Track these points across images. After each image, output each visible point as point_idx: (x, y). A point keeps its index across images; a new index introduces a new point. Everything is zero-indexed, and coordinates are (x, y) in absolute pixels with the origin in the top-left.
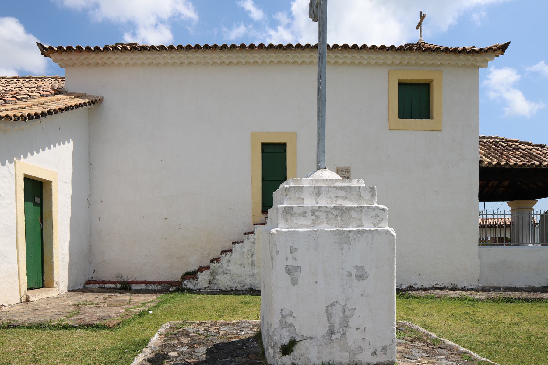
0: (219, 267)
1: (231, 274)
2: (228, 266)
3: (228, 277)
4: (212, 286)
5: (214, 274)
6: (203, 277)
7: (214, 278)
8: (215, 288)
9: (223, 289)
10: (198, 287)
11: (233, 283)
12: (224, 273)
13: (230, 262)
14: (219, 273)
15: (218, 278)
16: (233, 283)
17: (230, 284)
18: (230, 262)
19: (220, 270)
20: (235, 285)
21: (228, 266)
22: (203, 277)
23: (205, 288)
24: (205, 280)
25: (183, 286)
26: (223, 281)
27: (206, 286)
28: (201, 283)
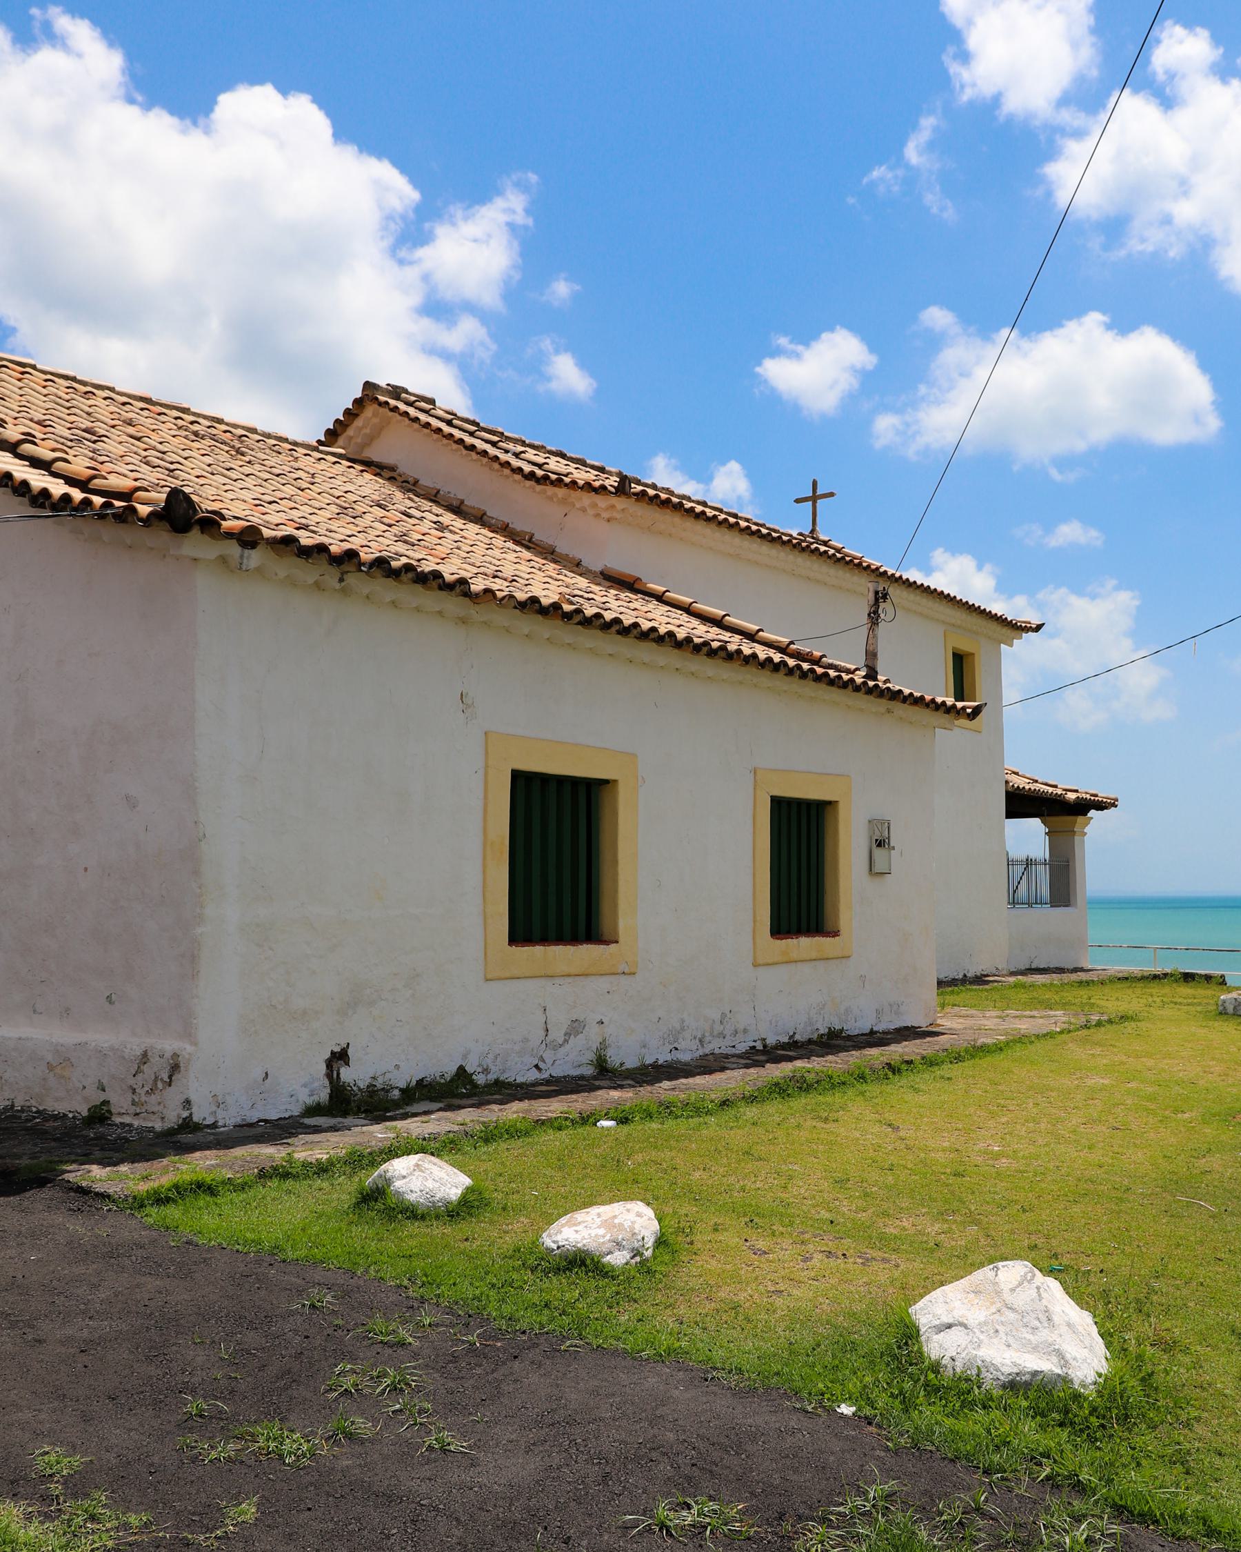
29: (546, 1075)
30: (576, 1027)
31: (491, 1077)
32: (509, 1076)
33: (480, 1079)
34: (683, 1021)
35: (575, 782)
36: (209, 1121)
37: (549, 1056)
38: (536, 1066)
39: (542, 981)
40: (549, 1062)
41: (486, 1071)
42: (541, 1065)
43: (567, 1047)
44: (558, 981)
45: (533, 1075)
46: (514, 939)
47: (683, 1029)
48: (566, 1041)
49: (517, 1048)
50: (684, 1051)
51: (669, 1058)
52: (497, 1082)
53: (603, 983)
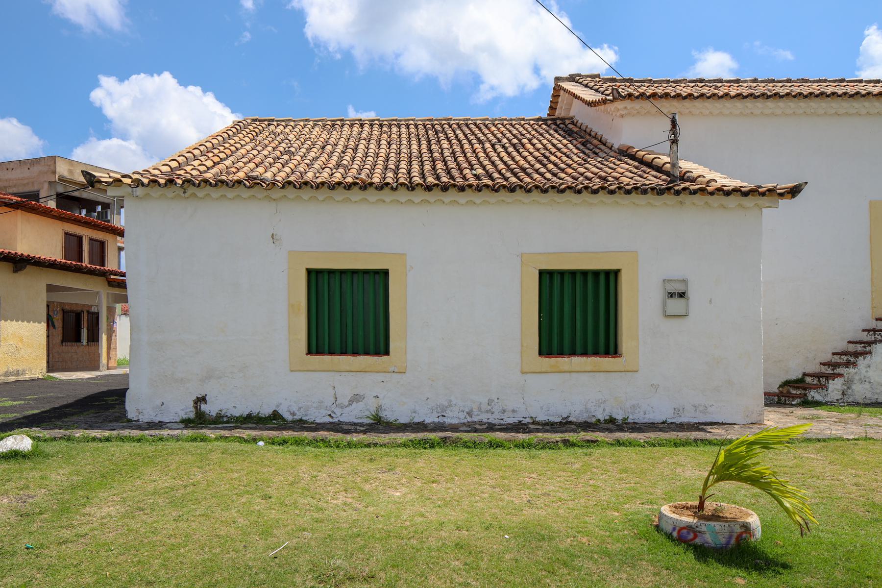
0: (856, 373)
1: (870, 382)
2: (867, 372)
3: (867, 386)
4: (846, 398)
5: (849, 383)
6: (835, 386)
7: (849, 388)
8: (850, 400)
9: (861, 401)
10: (828, 399)
11: (873, 394)
12: (862, 381)
13: (869, 366)
14: (856, 381)
15: (853, 387)
16: (873, 394)
17: (869, 395)
18: (869, 366)
19: (857, 377)
20: (876, 396)
21: (867, 372)
22: (835, 387)
23: (838, 400)
24: (837, 389)
25: (810, 398)
26: (860, 391)
27: (839, 398)
28: (832, 394)
29: (336, 420)
30: (357, 398)
31: (297, 417)
32: (310, 418)
33: (289, 417)
34: (450, 401)
35: (376, 272)
36: (136, 419)
37: (338, 411)
38: (330, 415)
39: (333, 373)
40: (338, 414)
41: (294, 414)
42: (333, 415)
43: (351, 408)
44: (344, 374)
45: (328, 420)
46: (309, 352)
47: (450, 406)
48: (350, 405)
49: (315, 405)
50: (452, 418)
51: (436, 420)
52: (301, 420)
53: (380, 377)
